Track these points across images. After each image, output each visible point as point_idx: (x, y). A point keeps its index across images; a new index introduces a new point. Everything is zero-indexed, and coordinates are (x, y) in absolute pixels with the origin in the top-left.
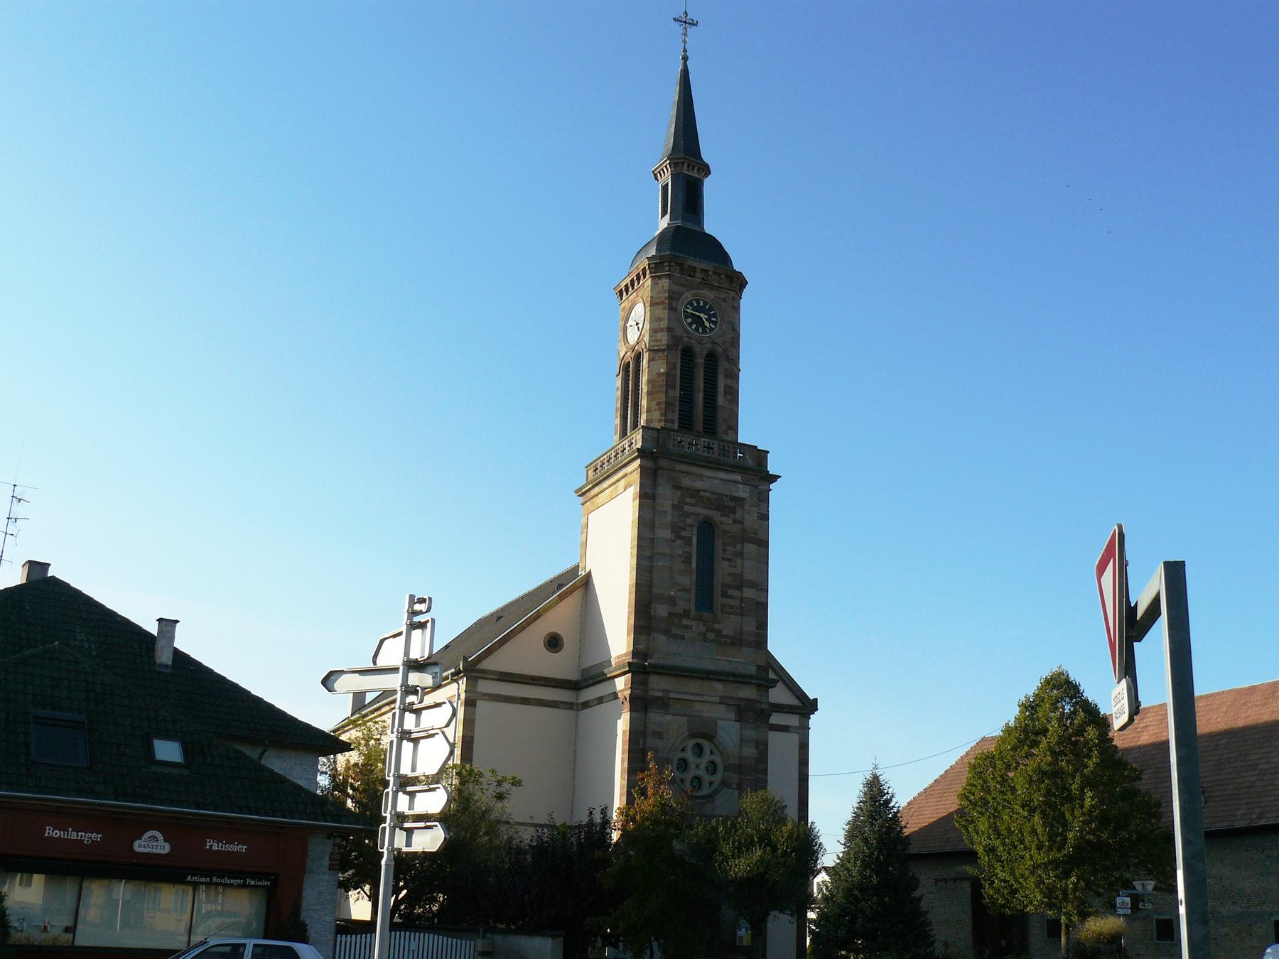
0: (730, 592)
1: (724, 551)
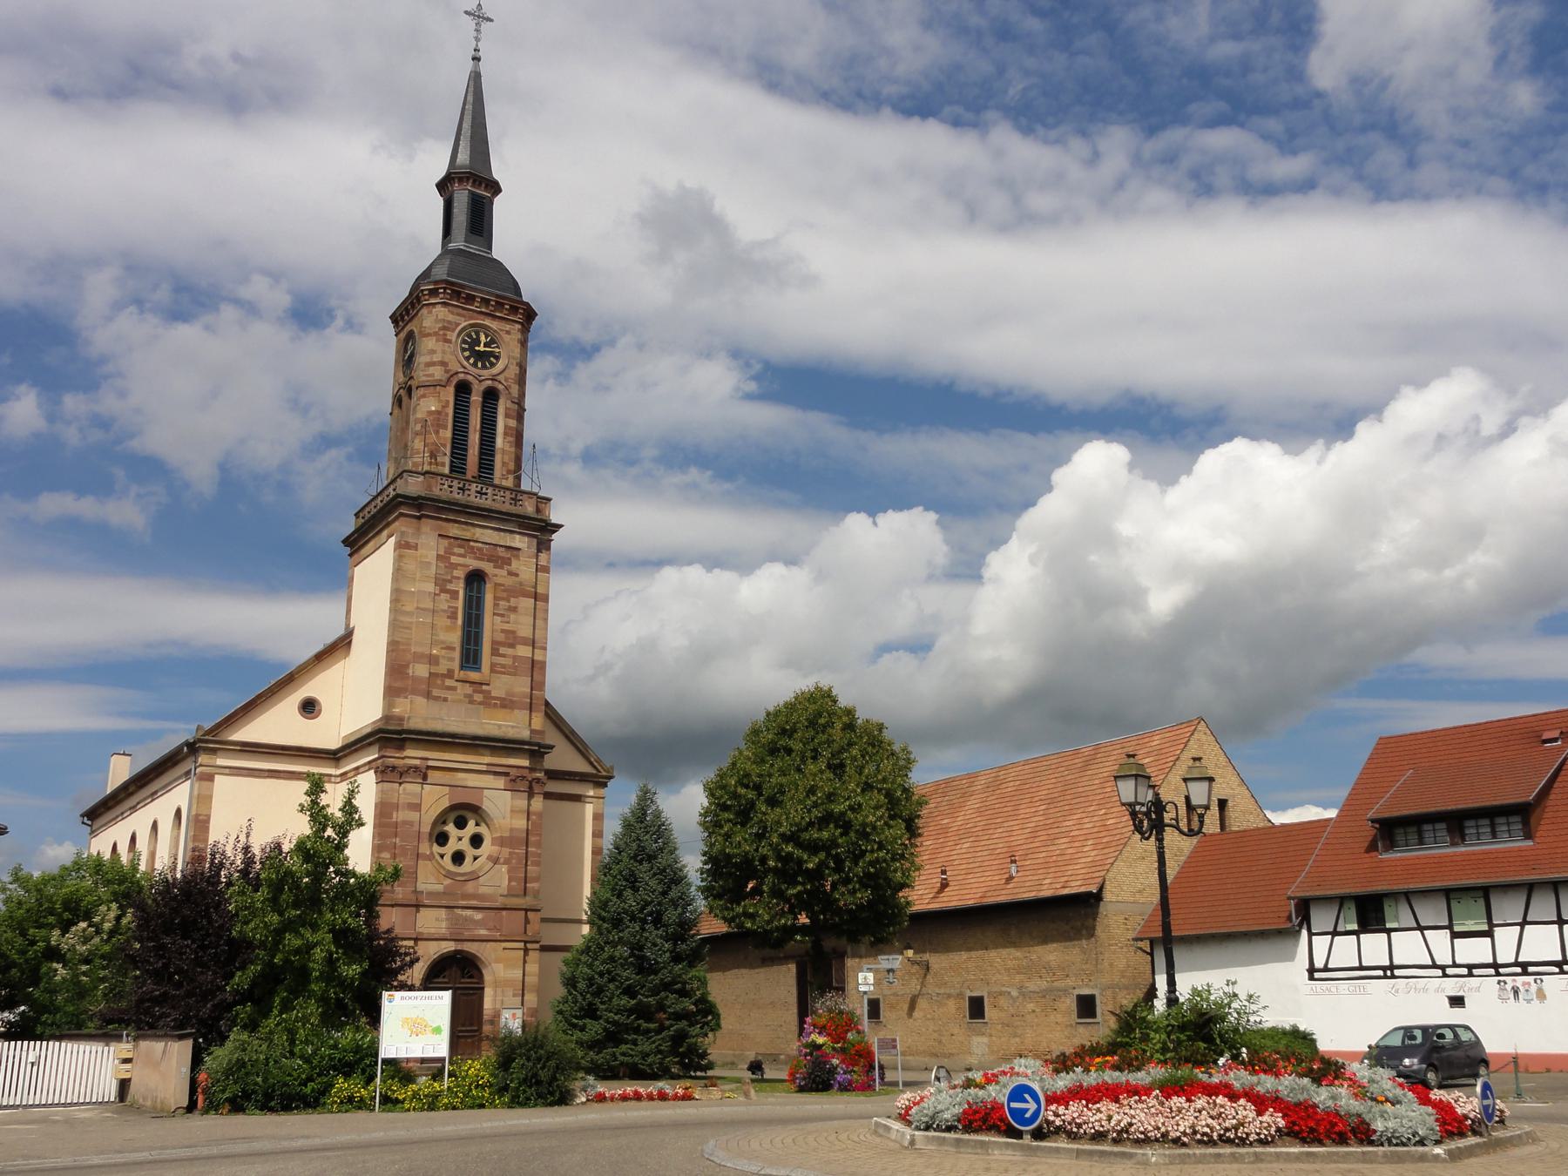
0: (502, 650)
1: (496, 605)
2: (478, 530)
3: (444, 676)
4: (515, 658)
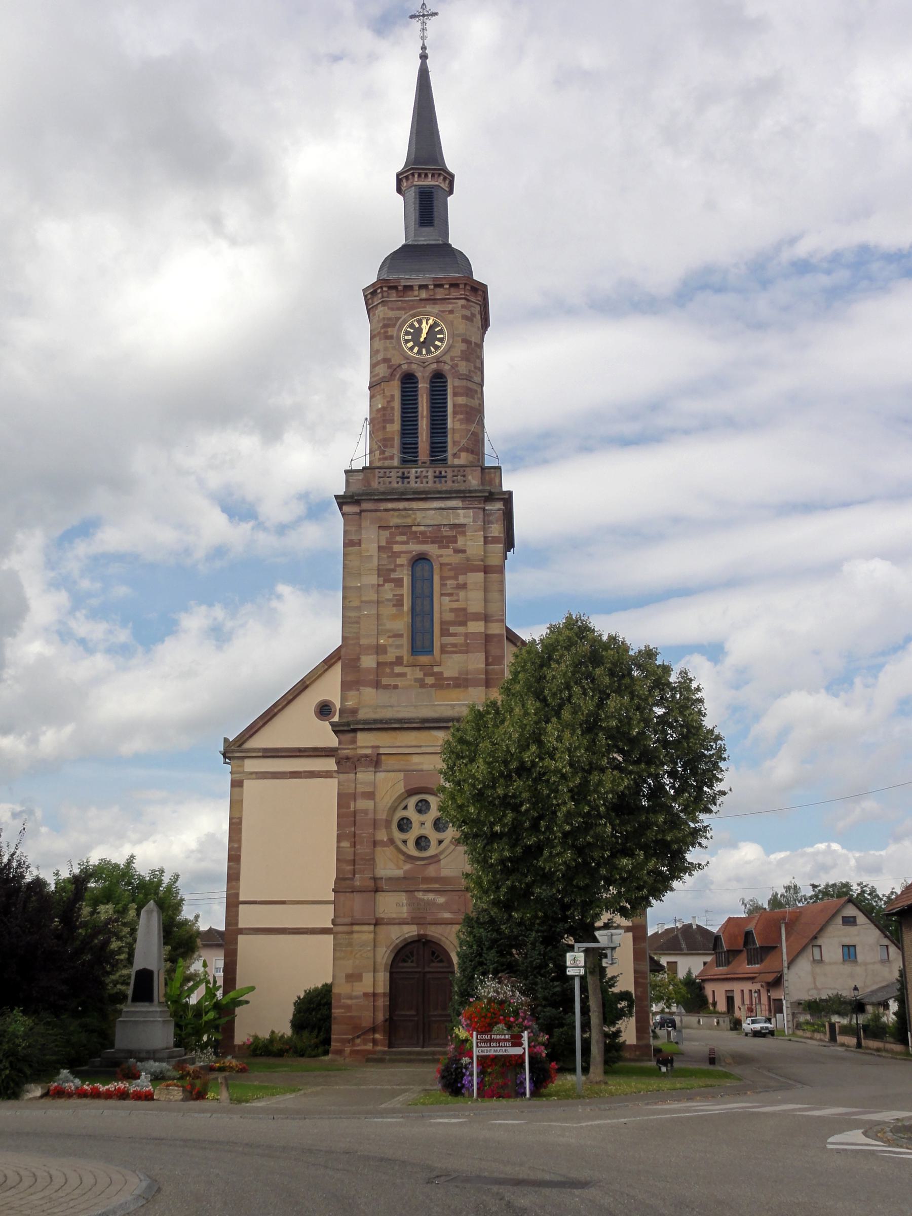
0: (452, 630)
1: (443, 585)
2: (419, 515)
3: (392, 664)
4: (466, 635)
